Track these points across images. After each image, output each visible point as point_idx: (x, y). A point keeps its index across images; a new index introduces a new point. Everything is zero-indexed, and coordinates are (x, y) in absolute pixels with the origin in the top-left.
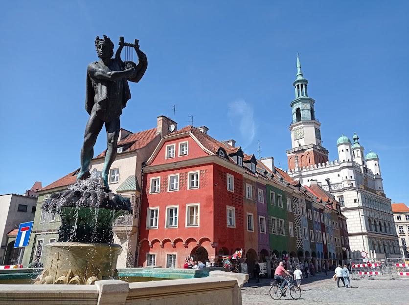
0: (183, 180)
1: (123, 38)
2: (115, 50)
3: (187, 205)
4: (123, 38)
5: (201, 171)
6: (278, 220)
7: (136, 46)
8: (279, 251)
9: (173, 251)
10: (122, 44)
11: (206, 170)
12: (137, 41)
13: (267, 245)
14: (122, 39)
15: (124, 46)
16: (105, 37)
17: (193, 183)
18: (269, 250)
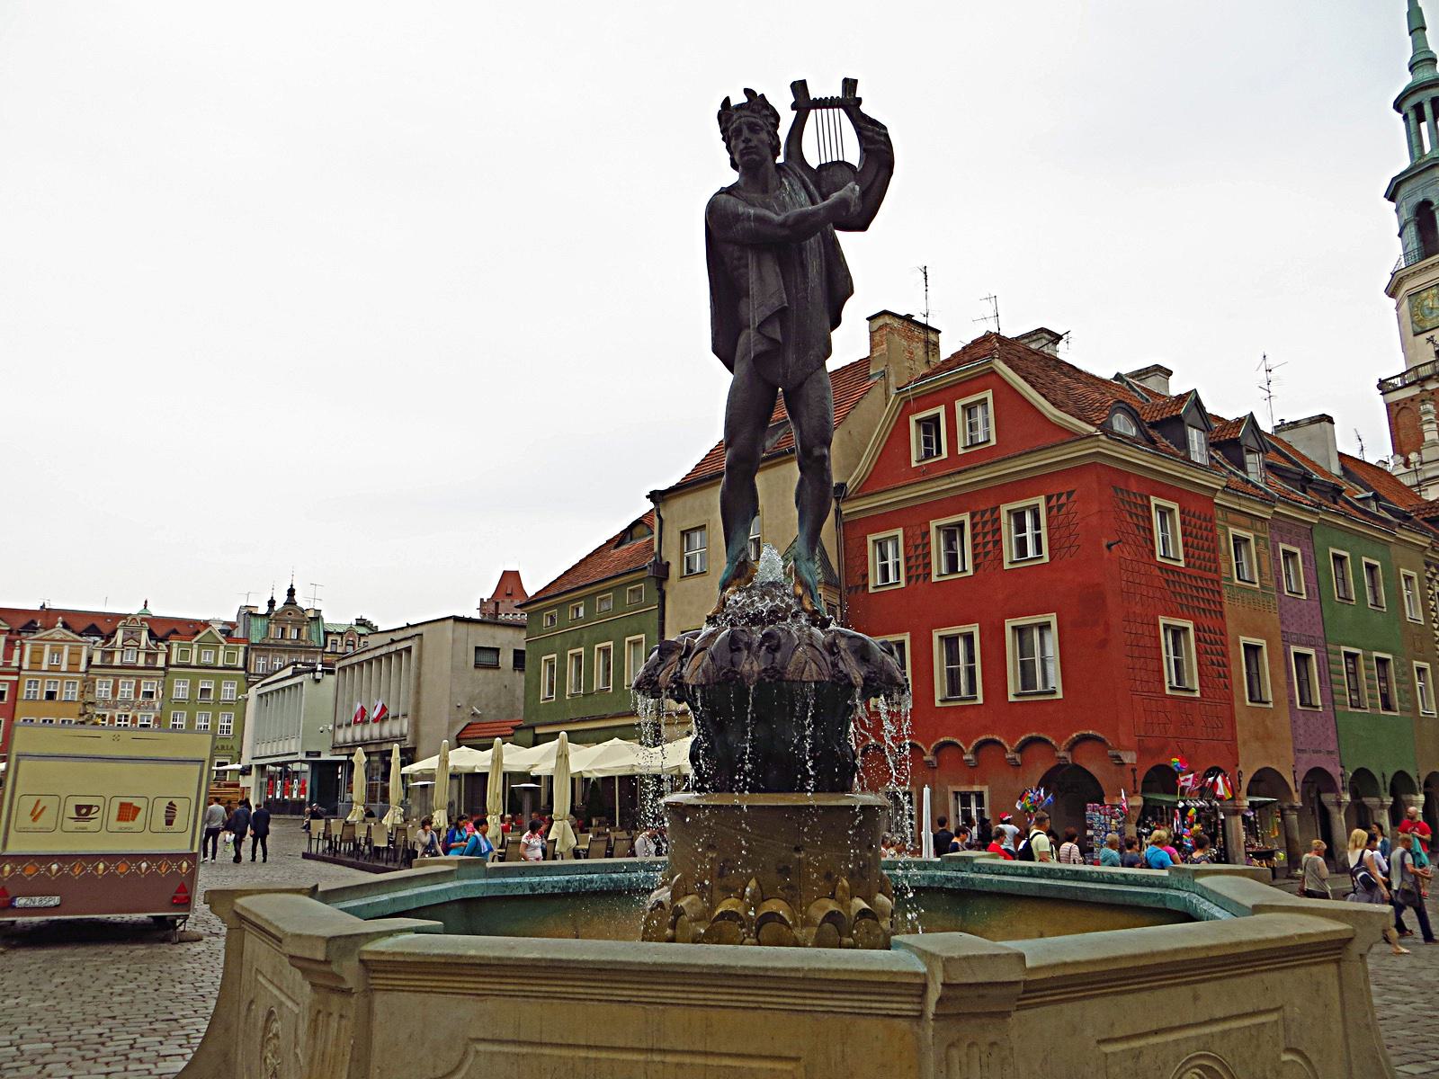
0: (985, 535)
1: (803, 83)
2: (783, 132)
3: (1009, 624)
4: (803, 83)
5: (1048, 499)
6: (1368, 659)
7: (849, 100)
8: (1378, 776)
9: (972, 783)
10: (803, 100)
11: (1070, 494)
12: (850, 85)
13: (1330, 752)
14: (799, 88)
15: (812, 112)
16: (748, 92)
17: (1022, 544)
18: (1334, 770)
